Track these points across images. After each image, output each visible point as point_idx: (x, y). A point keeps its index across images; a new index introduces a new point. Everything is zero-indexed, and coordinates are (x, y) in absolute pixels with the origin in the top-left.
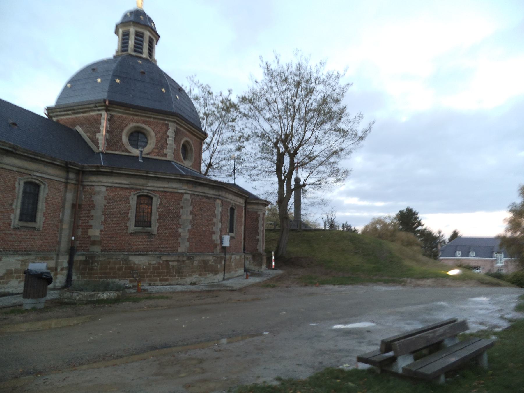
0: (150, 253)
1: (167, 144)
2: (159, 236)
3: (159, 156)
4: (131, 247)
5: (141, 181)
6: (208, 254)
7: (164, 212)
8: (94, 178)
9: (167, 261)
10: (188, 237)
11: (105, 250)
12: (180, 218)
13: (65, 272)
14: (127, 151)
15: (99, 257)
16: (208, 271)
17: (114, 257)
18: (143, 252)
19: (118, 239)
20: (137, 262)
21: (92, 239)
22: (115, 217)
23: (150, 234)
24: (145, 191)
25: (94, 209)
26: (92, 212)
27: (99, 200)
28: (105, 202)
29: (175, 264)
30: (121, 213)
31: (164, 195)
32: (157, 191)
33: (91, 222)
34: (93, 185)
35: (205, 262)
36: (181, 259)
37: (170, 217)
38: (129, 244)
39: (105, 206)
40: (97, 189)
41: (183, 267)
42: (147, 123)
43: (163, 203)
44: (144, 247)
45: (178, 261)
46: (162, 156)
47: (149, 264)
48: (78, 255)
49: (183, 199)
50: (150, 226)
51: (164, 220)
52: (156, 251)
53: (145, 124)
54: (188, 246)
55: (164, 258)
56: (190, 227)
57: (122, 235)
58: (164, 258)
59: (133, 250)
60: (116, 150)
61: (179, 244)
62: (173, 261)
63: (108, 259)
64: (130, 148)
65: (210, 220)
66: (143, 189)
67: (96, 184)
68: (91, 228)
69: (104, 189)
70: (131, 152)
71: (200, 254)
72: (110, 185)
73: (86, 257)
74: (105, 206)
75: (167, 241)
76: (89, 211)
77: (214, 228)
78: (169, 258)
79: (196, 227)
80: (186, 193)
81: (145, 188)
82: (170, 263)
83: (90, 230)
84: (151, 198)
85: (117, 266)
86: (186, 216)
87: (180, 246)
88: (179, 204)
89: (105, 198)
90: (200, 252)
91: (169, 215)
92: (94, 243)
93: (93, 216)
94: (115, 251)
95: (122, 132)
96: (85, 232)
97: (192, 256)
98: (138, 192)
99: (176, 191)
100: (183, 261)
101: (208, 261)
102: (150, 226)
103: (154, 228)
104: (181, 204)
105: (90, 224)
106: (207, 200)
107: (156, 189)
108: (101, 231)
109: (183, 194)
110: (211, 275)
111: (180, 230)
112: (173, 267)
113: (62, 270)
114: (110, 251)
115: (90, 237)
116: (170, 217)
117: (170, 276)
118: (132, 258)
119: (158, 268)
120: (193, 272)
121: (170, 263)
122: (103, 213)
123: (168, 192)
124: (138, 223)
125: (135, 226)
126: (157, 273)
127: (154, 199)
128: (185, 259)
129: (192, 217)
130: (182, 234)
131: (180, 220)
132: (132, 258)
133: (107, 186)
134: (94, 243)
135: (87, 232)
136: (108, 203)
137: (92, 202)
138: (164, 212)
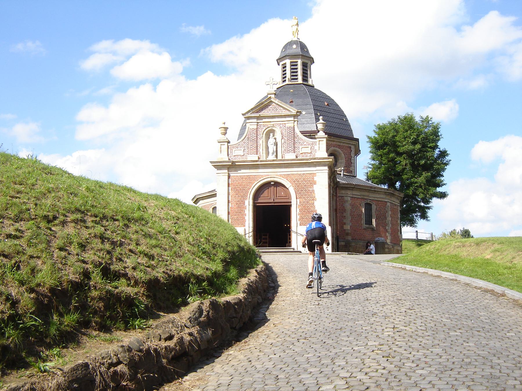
5: (366, 194)
8: (343, 192)
24: (369, 200)
26: (345, 214)
27: (348, 207)
37: (382, 219)
40: (346, 198)
42: (339, 147)
43: (378, 208)
49: (387, 206)
51: (379, 220)
53: (338, 148)
67: (345, 195)
69: (349, 199)
72: (352, 196)
80: (388, 202)
81: (368, 198)
84: (371, 205)
86: (389, 219)
88: (385, 209)
99: (383, 200)
109: (386, 202)
116: (382, 219)
127: (373, 206)
130: (388, 230)
131: (386, 220)
133: (351, 197)
137: (344, 207)
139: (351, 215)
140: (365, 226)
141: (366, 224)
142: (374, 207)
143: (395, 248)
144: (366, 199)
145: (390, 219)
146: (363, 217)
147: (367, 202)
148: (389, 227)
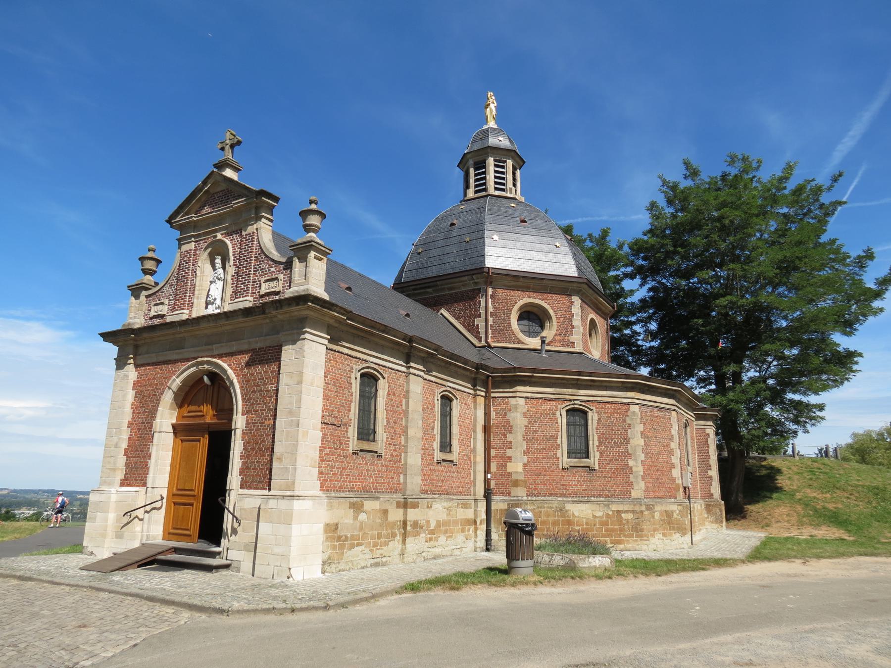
0: (592, 498)
1: (573, 327)
2: (602, 472)
3: (563, 345)
4: (566, 489)
6: (670, 500)
7: (605, 434)
9: (618, 512)
10: (642, 473)
11: (532, 495)
12: (629, 444)
13: (484, 526)
14: (520, 342)
15: (527, 504)
16: (674, 529)
17: (546, 506)
18: (582, 497)
19: (547, 478)
20: (576, 514)
21: (514, 477)
22: (540, 444)
23: (591, 469)
24: (579, 403)
25: (511, 433)
26: (510, 437)
28: (525, 422)
29: (630, 516)
30: (548, 437)
31: (602, 408)
32: (592, 402)
33: (509, 453)
34: (507, 397)
35: (669, 514)
36: (637, 508)
38: (563, 485)
39: (526, 426)
41: (643, 521)
43: (603, 419)
44: (583, 490)
45: (633, 512)
46: (568, 346)
47: (595, 517)
48: (497, 501)
49: (629, 413)
50: (588, 457)
52: (600, 496)
53: (540, 299)
54: (643, 488)
55: (614, 507)
56: (643, 457)
57: (552, 471)
58: (614, 507)
59: (569, 494)
60: (504, 342)
61: (631, 485)
62: (627, 512)
63: (538, 507)
64: (521, 336)
65: (667, 446)
66: (574, 400)
68: (511, 462)
69: (522, 402)
70: (525, 342)
71: (659, 500)
72: (529, 395)
73: (509, 505)
74: (526, 426)
75: (614, 480)
76: (505, 435)
77: (673, 458)
78: (621, 508)
79: (651, 457)
82: (623, 515)
83: (508, 464)
84: (585, 413)
85: (551, 519)
86: (637, 441)
87: (633, 489)
88: (624, 421)
89: (525, 416)
90: (660, 498)
91: (612, 439)
92: (516, 484)
93: (511, 442)
94: (545, 496)
95: (510, 313)
96: (502, 467)
97: (652, 503)
98: (567, 404)
100: (642, 512)
101: (672, 512)
102: (588, 457)
103: (594, 460)
104: (628, 421)
105: (508, 455)
106: (659, 414)
107: (591, 398)
108: (525, 466)
110: (678, 535)
111: (631, 463)
112: (627, 521)
113: (481, 524)
114: (538, 496)
115: (510, 474)
117: (625, 536)
118: (569, 507)
119: (606, 523)
120: (655, 530)
121: (623, 515)
122: (524, 438)
123: (608, 403)
124: (571, 453)
125: (569, 457)
126: (607, 530)
127: (590, 414)
128: (643, 508)
129: (645, 441)
130: (634, 469)
132: (569, 507)
134: (516, 484)
135: (505, 466)
136: (529, 422)
137: (508, 421)
138: (605, 434)
139: (525, 438)
140: (566, 461)
141: (569, 457)
142: (593, 417)
143: (658, 508)
144: (570, 400)
145: (642, 442)
146: (563, 440)
147: (573, 406)
148: (636, 460)
